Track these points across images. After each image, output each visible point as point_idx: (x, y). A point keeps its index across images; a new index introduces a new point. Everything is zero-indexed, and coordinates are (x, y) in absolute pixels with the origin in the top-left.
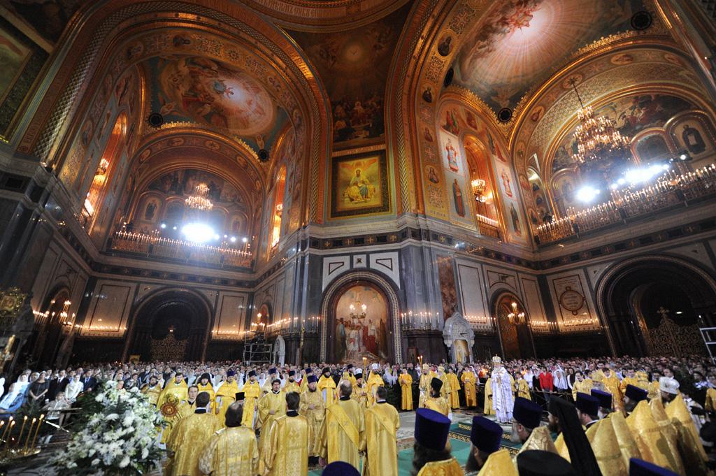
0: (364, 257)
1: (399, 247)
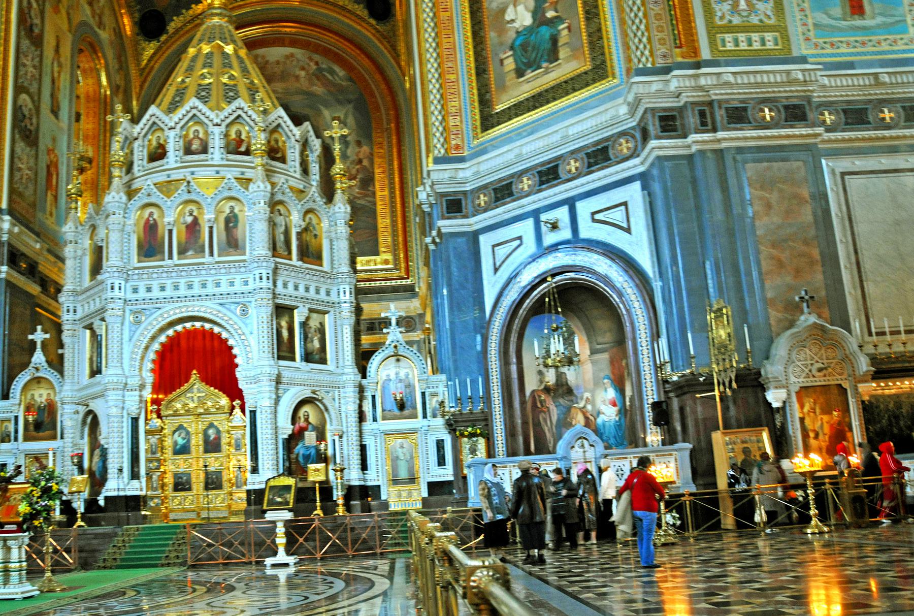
0: (562, 214)
1: (642, 169)
